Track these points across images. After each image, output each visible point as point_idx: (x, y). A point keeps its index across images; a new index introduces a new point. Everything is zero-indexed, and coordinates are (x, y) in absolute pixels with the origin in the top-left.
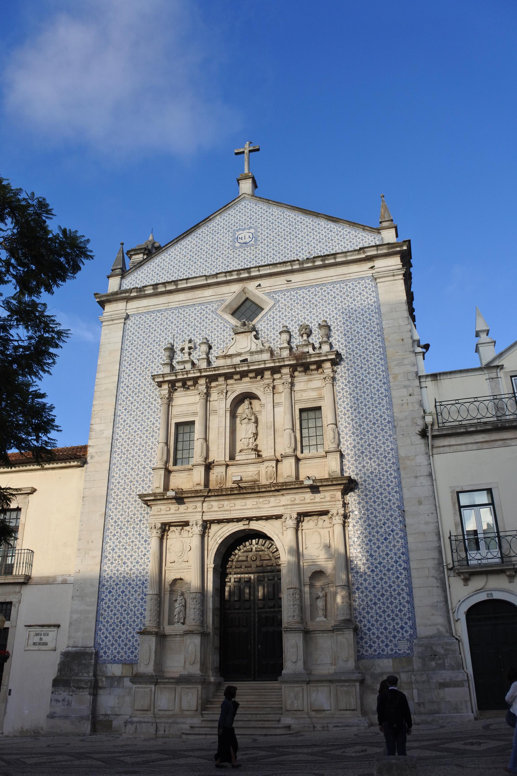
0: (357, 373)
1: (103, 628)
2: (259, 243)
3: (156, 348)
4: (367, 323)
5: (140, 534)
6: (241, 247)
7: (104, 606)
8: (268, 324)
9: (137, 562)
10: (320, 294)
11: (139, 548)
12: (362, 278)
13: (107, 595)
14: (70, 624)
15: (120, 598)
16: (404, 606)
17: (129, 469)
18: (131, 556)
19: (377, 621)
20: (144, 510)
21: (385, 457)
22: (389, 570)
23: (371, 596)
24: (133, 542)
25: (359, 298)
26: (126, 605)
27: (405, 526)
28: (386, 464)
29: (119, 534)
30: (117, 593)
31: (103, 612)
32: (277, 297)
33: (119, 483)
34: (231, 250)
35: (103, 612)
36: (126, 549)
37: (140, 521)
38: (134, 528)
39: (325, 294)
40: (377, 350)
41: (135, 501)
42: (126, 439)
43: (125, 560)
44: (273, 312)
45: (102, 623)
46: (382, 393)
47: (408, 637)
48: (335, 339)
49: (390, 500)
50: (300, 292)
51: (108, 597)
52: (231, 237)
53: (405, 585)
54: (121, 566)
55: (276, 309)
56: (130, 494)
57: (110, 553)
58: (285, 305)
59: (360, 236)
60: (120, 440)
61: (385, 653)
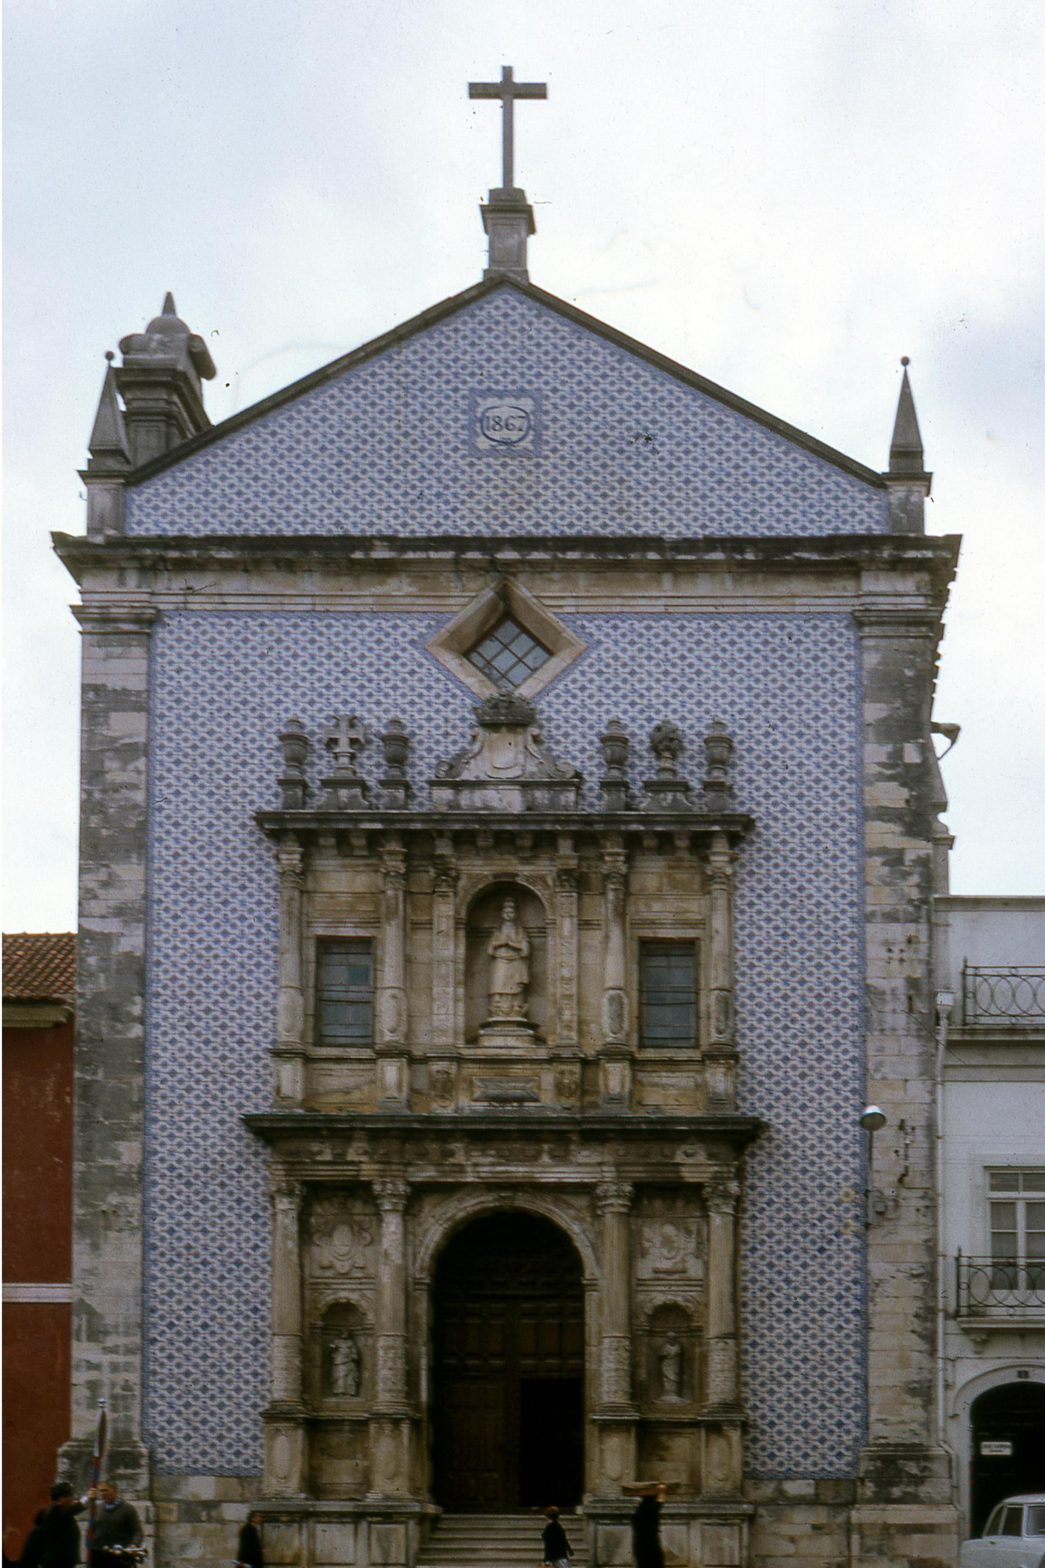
0: (789, 870)
2: (546, 450)
3: (253, 725)
4: (825, 742)
5: (239, 1201)
6: (493, 452)
8: (567, 704)
10: (710, 640)
11: (239, 1232)
12: (825, 616)
16: (848, 1385)
17: (197, 1042)
18: (221, 1248)
19: (789, 1408)
20: (248, 1146)
21: (837, 1075)
22: (822, 1312)
23: (781, 1361)
25: (811, 671)
26: (216, 1355)
28: (837, 1091)
32: (594, 630)
33: (173, 1073)
34: (463, 457)
36: (205, 1231)
37: (239, 1170)
38: (222, 1185)
39: (724, 642)
40: (843, 819)
41: (222, 1122)
42: (182, 963)
43: (204, 1255)
44: (583, 673)
46: (844, 928)
47: (851, 1443)
48: (742, 773)
49: (838, 1171)
50: (658, 627)
52: (464, 412)
53: (856, 1344)
55: (591, 665)
56: (206, 1105)
58: (616, 658)
59: (832, 486)
60: (167, 964)
61: (801, 1469)
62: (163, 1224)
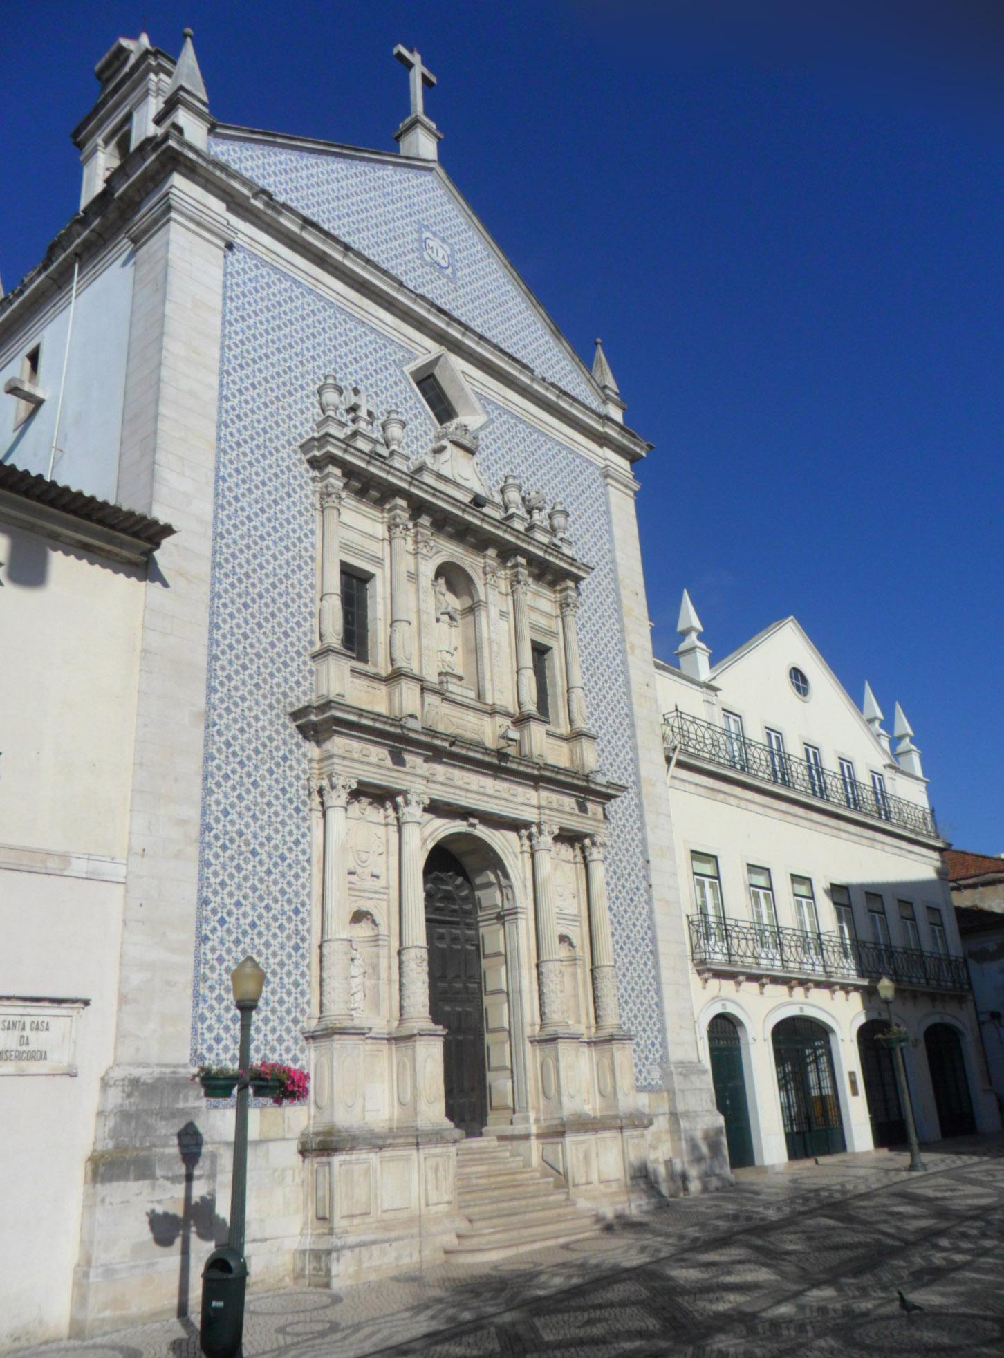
1: (208, 1014)
5: (284, 791)
7: (209, 956)
9: (283, 858)
13: (214, 930)
14: (123, 999)
15: (247, 940)
18: (269, 839)
24: (269, 804)
27: (650, 886)
29: (237, 777)
30: (239, 926)
31: (207, 971)
35: (207, 971)
38: (271, 772)
45: (205, 1001)
51: (219, 934)
54: (247, 861)
57: (217, 820)
62: (218, 803)
